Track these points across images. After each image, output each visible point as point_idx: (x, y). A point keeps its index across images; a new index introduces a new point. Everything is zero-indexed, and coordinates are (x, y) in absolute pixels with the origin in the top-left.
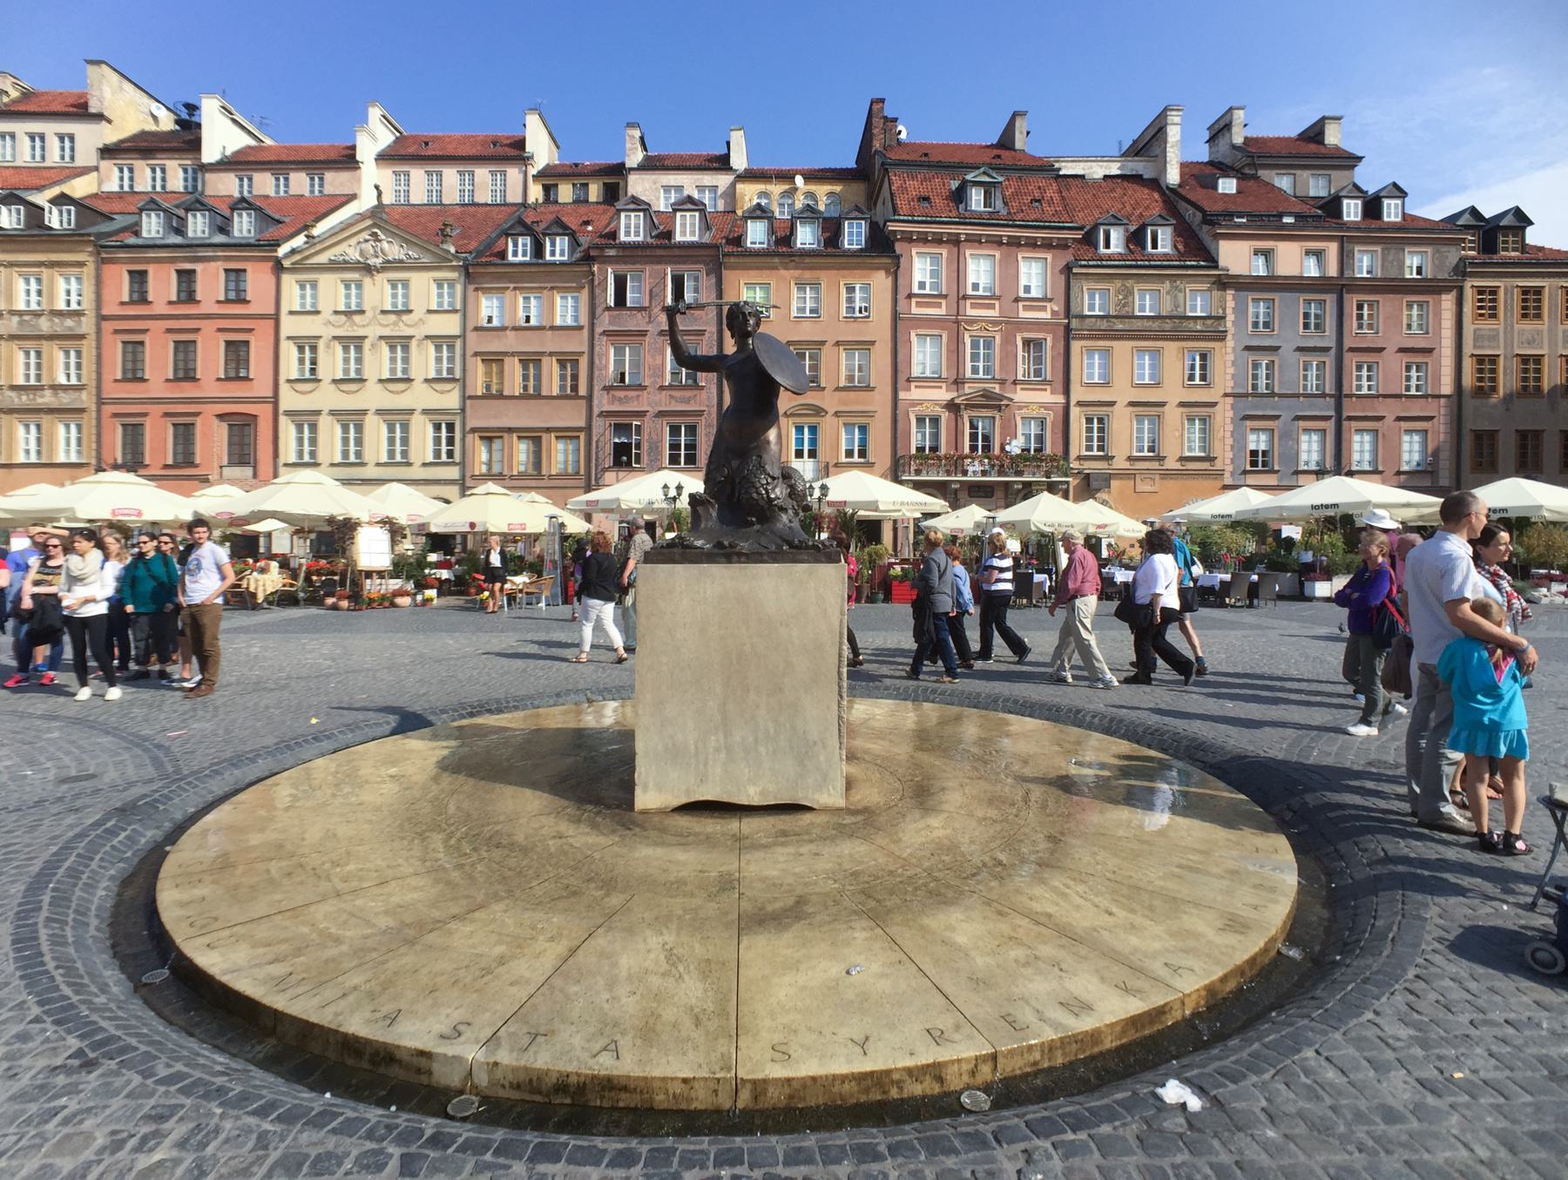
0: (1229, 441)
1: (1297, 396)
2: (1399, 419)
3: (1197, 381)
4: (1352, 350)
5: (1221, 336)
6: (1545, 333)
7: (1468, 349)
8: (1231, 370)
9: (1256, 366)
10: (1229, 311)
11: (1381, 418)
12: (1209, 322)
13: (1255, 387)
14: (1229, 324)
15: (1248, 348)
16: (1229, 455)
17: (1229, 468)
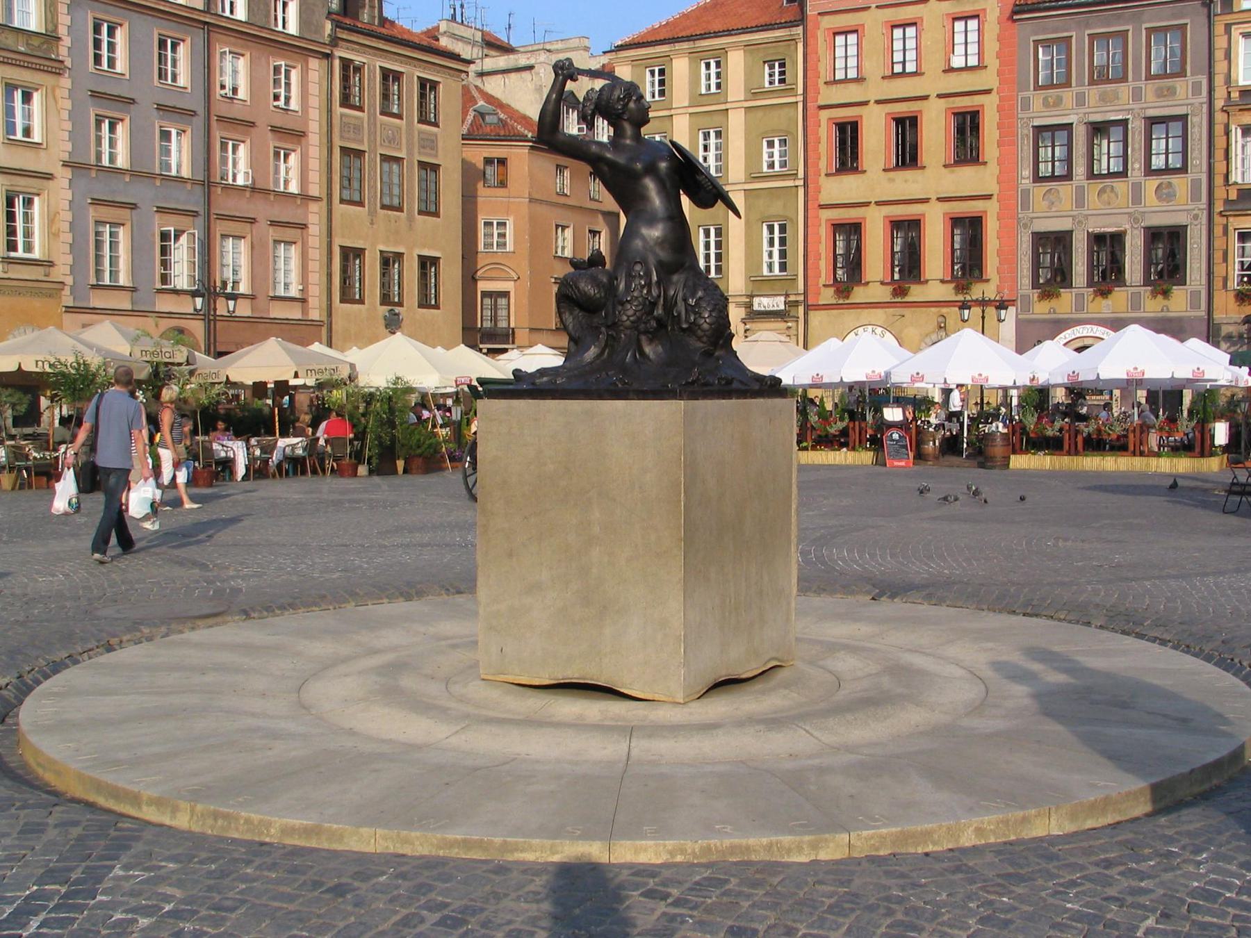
0: (68, 238)
1: (152, 176)
2: (273, 223)
3: (19, 136)
4: (221, 119)
5: (56, 68)
6: (404, 128)
7: (338, 143)
8: (69, 126)
9: (99, 123)
10: (62, 31)
11: (253, 221)
12: (36, 42)
13: (99, 156)
14: (63, 52)
15: (95, 95)
16: (70, 259)
17: (69, 280)
